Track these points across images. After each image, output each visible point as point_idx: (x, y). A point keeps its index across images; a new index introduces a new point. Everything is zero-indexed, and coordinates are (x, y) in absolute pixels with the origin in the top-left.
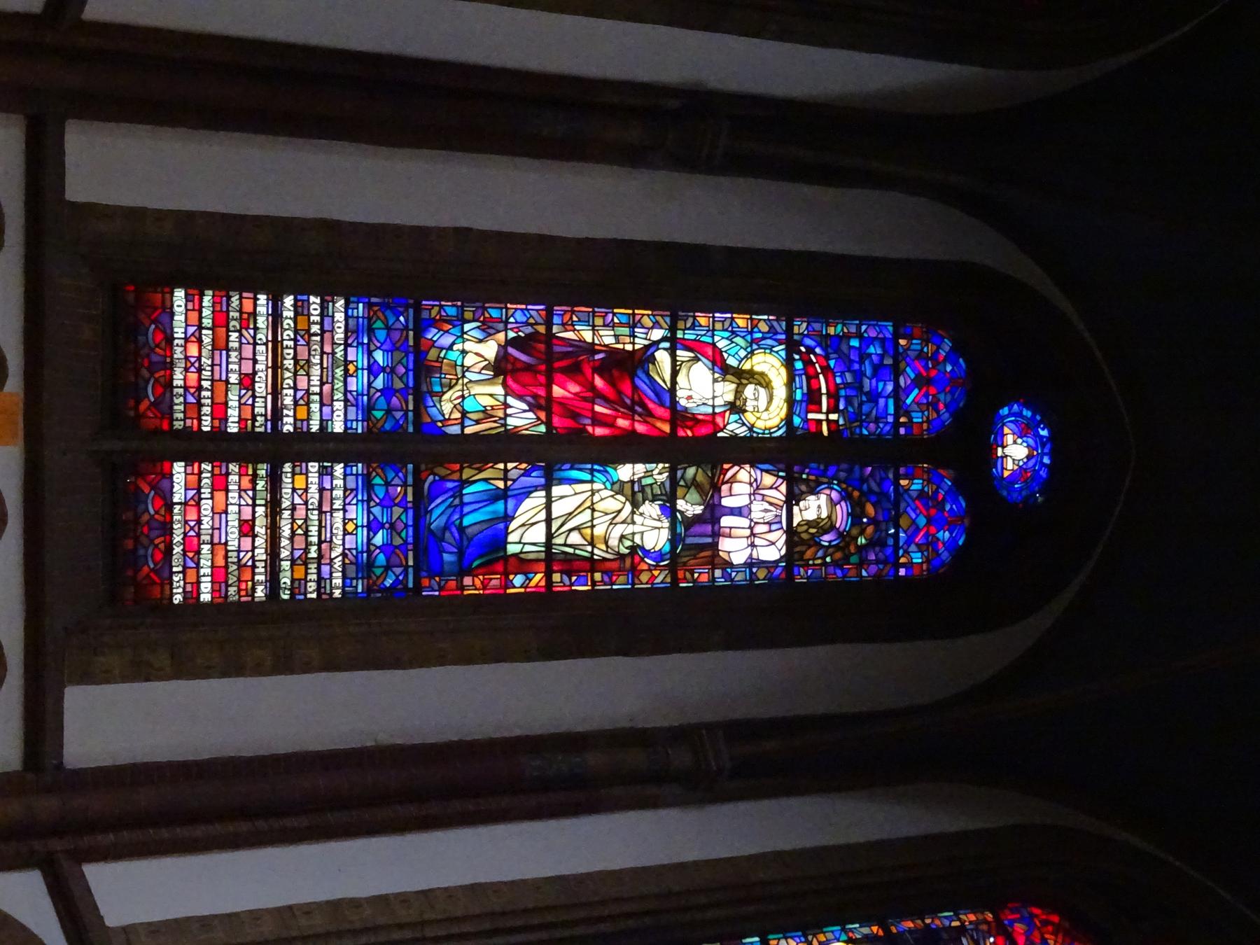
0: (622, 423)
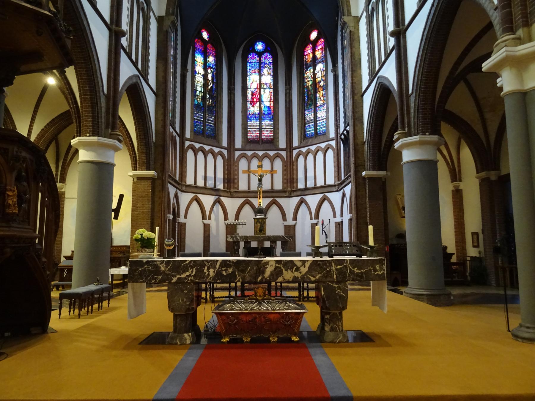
0: (258, 94)
